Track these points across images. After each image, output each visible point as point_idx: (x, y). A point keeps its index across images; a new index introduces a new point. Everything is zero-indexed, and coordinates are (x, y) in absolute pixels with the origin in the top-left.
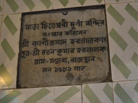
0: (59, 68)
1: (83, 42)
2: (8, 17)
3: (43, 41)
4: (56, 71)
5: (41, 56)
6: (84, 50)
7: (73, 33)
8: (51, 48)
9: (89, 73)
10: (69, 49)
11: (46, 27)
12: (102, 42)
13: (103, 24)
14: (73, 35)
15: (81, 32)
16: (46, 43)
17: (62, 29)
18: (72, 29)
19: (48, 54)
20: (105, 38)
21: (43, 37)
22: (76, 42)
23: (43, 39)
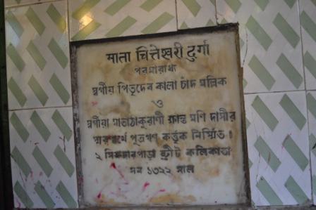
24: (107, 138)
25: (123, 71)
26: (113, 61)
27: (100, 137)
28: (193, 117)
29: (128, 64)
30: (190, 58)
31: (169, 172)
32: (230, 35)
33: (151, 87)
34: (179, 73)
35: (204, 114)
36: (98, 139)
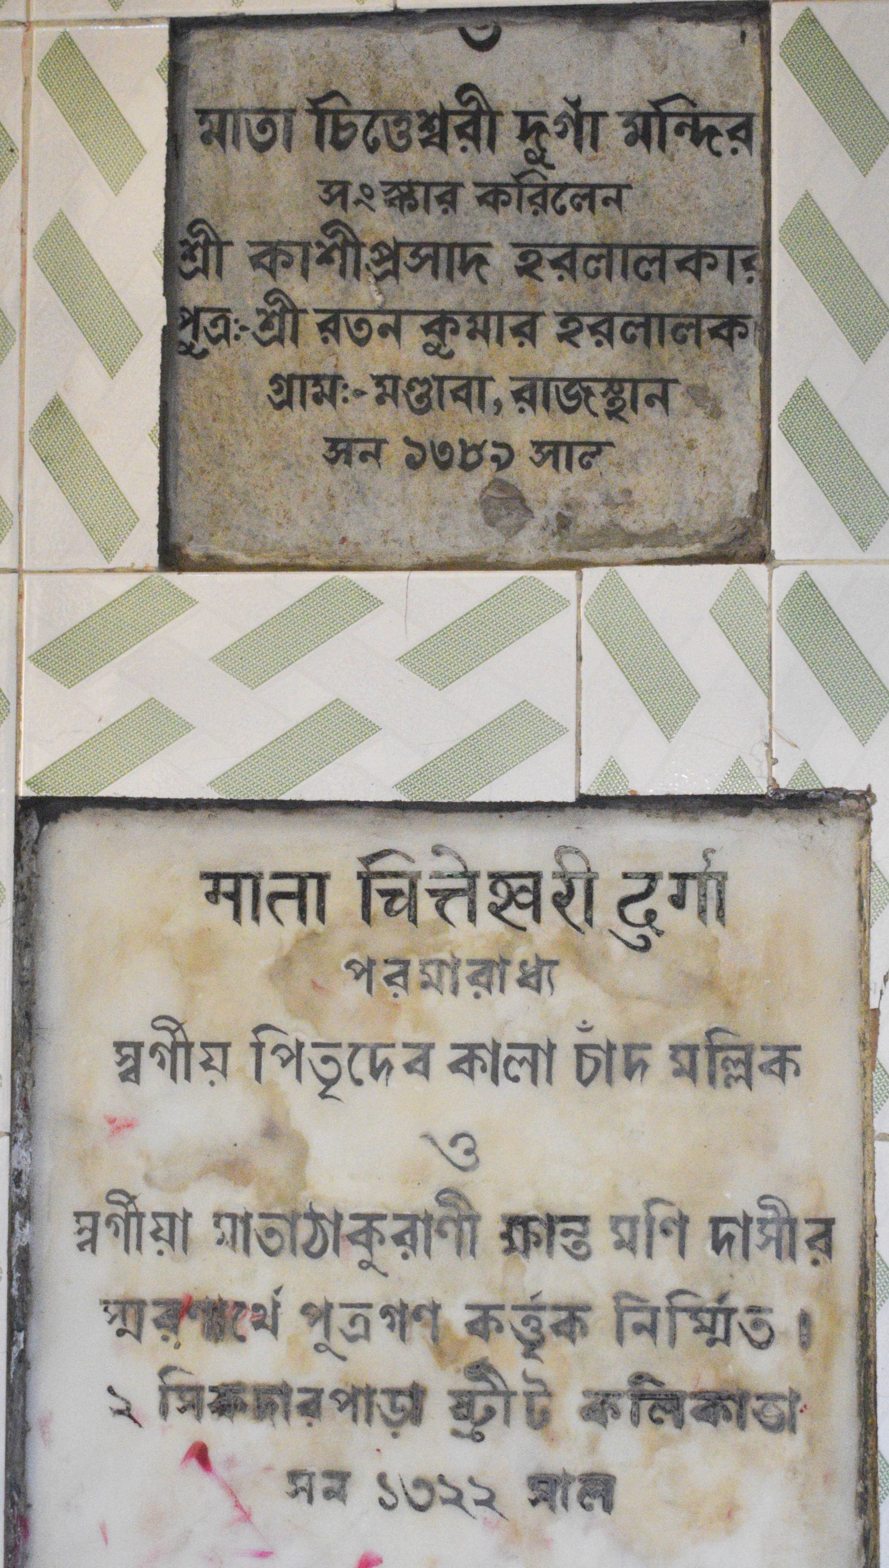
0: (432, 444)
1: (597, 271)
2: (66, 43)
3: (328, 242)
4: (413, 464)
5: (310, 354)
6: (604, 328)
7: (531, 200)
8: (379, 299)
9: (628, 492)
10: (501, 315)
11: (343, 135)
12: (730, 276)
13: (748, 141)
14: (535, 213)
15: (591, 197)
16: (344, 257)
17: (458, 162)
18: (529, 167)
19: (361, 342)
20: (749, 253)
21: (325, 214)
22: (555, 264)
23: (324, 228)
24: (176, 1312)
25: (283, 968)
26: (237, 915)
27: (140, 1304)
28: (625, 1229)
29: (314, 934)
30: (630, 934)
31: (488, 1503)
32: (839, 834)
33: (425, 1059)
34: (569, 1007)
35: (683, 1220)
36: (126, 1314)
